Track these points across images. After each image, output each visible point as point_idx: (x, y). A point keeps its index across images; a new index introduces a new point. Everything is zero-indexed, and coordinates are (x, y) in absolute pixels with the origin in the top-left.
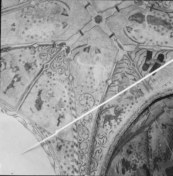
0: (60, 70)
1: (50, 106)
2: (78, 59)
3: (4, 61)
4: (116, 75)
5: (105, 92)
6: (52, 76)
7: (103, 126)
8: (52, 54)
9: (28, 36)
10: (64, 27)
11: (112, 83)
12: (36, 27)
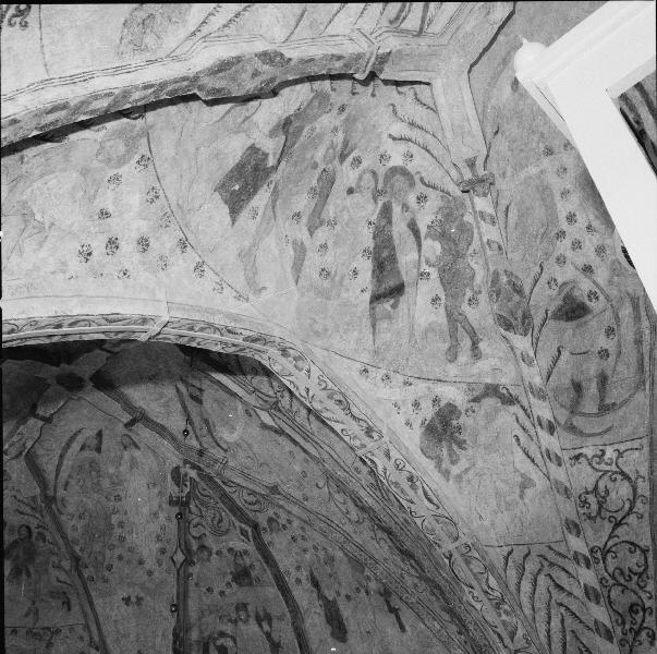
9: (160, 563)
10: (137, 447)
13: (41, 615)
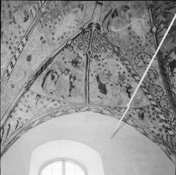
0: (103, 48)
1: (114, 85)
2: (113, 28)
3: (54, 71)
4: (158, 18)
5: (155, 42)
6: (99, 58)
8: (87, 40)
9: (59, 39)
11: (157, 29)
12: (59, 26)
13: (16, 13)
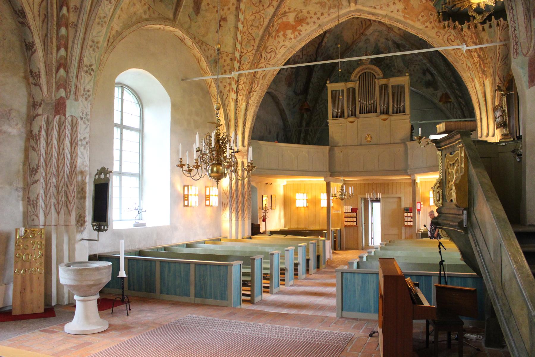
7: (275, 36)
